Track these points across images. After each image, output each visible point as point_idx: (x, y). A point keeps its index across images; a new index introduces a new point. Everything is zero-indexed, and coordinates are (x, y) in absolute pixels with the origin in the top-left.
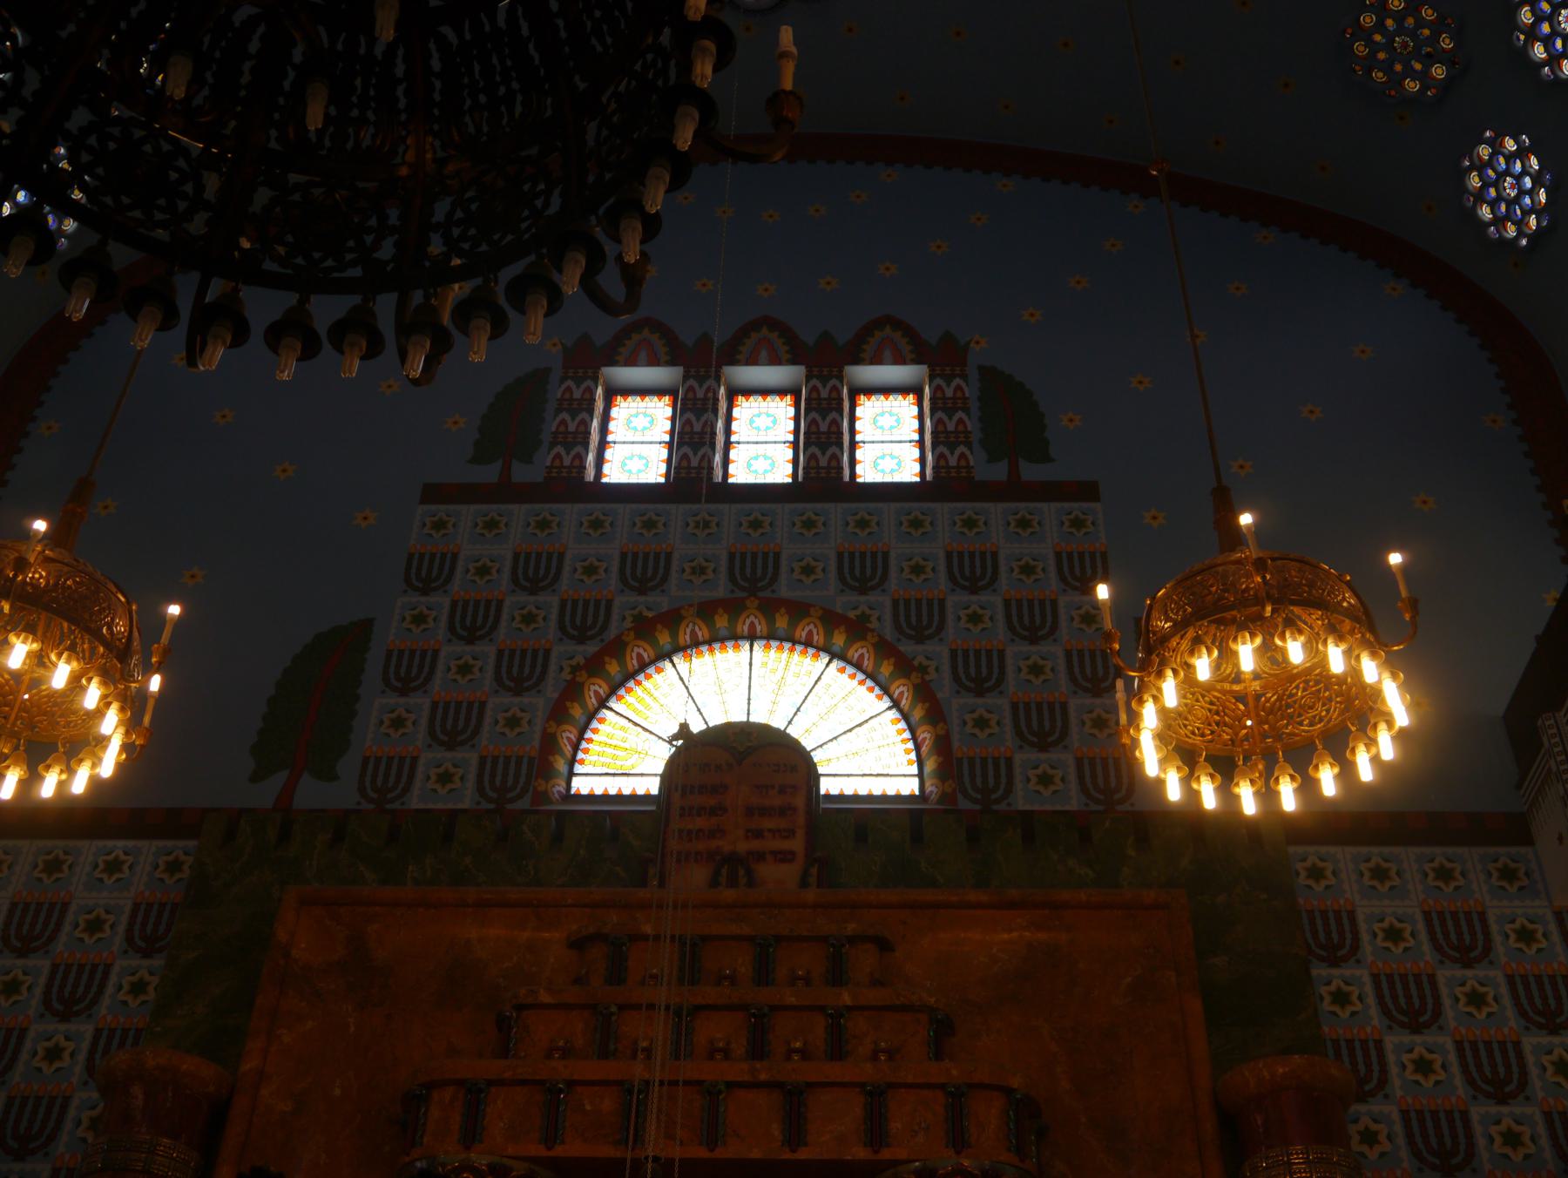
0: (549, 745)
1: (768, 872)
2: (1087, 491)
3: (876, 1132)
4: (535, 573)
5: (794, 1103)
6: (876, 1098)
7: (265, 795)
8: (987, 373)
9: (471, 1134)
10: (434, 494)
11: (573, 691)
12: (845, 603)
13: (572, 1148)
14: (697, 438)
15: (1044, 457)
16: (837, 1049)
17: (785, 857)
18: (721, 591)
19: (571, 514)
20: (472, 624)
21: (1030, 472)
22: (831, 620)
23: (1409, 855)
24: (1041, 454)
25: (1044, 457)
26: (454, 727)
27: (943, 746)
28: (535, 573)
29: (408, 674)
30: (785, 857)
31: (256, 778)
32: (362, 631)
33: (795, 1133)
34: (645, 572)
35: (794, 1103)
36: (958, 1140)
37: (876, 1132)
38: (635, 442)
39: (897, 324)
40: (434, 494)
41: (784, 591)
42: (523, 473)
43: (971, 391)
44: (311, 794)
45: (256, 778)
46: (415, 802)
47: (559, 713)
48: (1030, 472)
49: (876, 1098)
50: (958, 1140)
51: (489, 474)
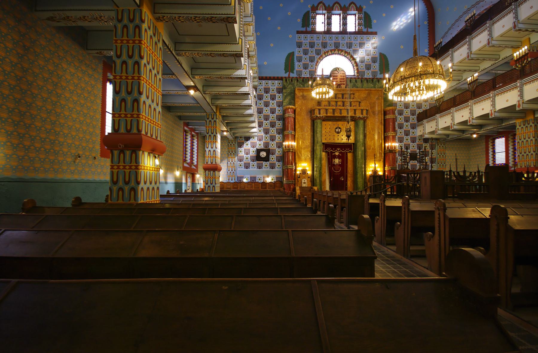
0: (316, 69)
1: (342, 86)
2: (375, 33)
4: (312, 45)
6: (355, 110)
7: (286, 75)
8: (365, 12)
9: (320, 114)
11: (317, 62)
15: (371, 28)
17: (344, 84)
18: (333, 48)
19: (315, 35)
20: (306, 52)
21: (370, 30)
22: (346, 52)
25: (371, 28)
26: (306, 67)
27: (358, 69)
28: (312, 45)
29: (299, 60)
30: (344, 84)
32: (293, 52)
34: (324, 45)
36: (362, 114)
37: (355, 114)
39: (354, 4)
40: (298, 32)
41: (340, 48)
42: (309, 29)
43: (363, 16)
44: (292, 75)
46: (303, 76)
47: (316, 65)
48: (370, 30)
49: (355, 110)
50: (362, 114)
51: (304, 29)
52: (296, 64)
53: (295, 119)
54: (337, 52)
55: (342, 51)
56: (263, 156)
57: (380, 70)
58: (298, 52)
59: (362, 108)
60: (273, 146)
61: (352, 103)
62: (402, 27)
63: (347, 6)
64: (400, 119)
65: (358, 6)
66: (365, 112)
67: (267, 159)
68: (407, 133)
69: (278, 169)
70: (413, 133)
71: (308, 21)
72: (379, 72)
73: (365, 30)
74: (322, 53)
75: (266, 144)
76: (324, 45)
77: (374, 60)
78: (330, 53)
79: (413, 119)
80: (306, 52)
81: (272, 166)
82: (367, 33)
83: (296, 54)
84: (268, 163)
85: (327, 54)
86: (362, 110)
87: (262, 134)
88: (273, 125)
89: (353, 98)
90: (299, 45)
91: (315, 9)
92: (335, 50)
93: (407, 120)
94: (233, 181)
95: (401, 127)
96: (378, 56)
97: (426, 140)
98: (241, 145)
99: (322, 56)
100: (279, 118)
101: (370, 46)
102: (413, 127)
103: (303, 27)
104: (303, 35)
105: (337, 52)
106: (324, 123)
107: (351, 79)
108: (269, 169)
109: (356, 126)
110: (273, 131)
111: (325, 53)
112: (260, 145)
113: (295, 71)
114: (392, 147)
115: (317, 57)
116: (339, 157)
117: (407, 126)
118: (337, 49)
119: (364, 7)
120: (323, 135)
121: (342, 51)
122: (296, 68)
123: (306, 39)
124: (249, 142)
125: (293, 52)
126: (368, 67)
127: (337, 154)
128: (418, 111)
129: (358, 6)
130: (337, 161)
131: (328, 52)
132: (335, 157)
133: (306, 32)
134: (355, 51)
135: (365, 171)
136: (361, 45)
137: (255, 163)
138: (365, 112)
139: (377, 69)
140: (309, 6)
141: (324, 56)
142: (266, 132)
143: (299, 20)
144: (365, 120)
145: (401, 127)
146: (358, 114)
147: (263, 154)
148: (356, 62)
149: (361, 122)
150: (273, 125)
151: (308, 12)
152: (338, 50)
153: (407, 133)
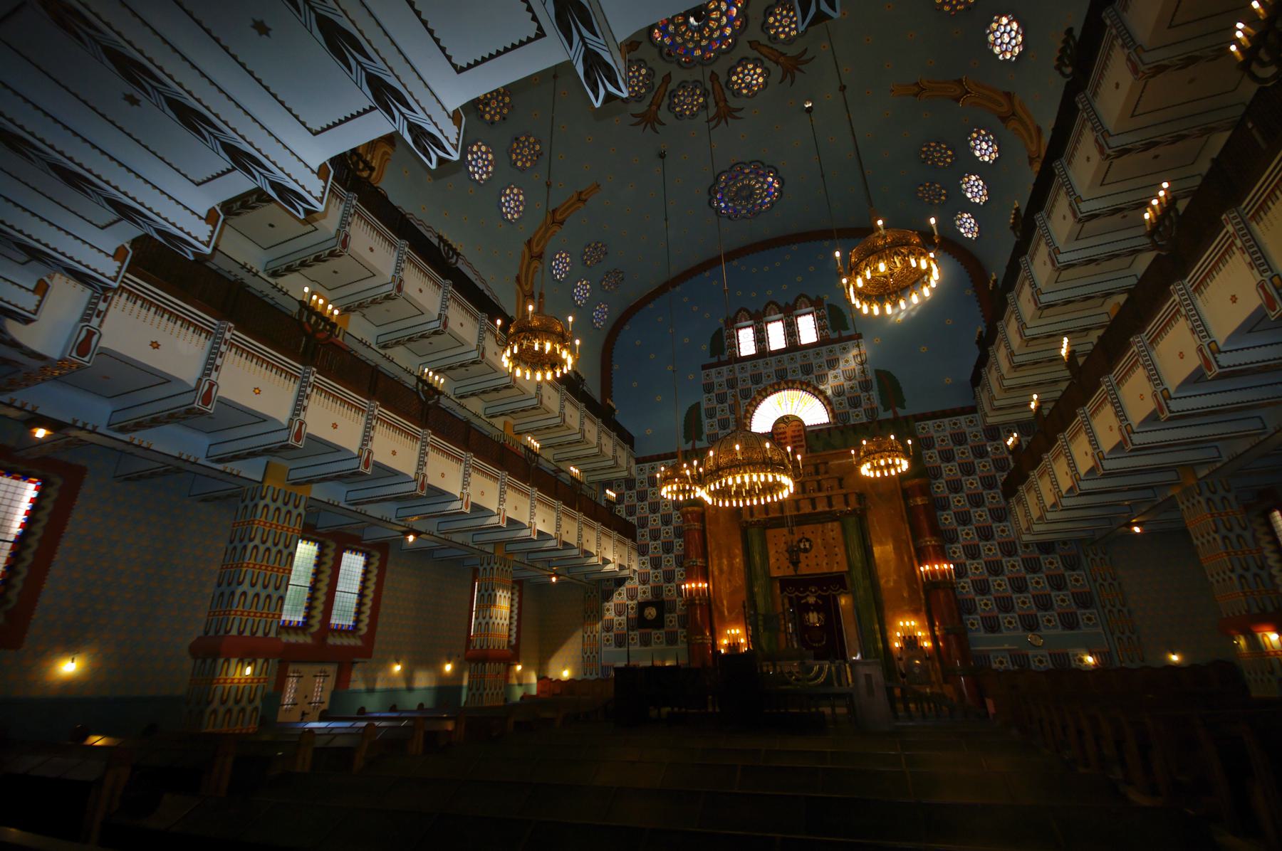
2: (859, 336)
3: (830, 505)
4: (732, 384)
5: (813, 502)
6: (829, 498)
7: (689, 447)
8: (829, 305)
10: (704, 367)
12: (804, 378)
13: (771, 515)
14: (761, 338)
15: (846, 328)
16: (820, 490)
21: (844, 333)
22: (802, 383)
23: (946, 420)
24: (846, 328)
27: (832, 411)
29: (711, 413)
31: (687, 442)
32: (697, 406)
33: (814, 507)
34: (757, 379)
35: (813, 502)
36: (847, 504)
37: (830, 505)
38: (746, 343)
40: (704, 367)
42: (724, 358)
45: (687, 442)
48: (844, 333)
49: (829, 498)
50: (847, 504)
51: (714, 360)
52: (706, 422)
53: (703, 532)
54: (783, 385)
55: (794, 382)
56: (649, 617)
57: (882, 403)
58: (705, 402)
59: (844, 491)
60: (668, 592)
61: (824, 482)
62: (913, 314)
63: (791, 303)
64: (958, 501)
65: (814, 298)
66: (853, 499)
67: (658, 623)
68: (986, 534)
69: (681, 646)
70: (1003, 531)
71: (723, 343)
72: (881, 409)
73: (835, 335)
74: (754, 394)
75: (657, 591)
76: (757, 379)
77: (865, 386)
78: (770, 390)
79: (993, 497)
80: (721, 399)
81: (671, 639)
82: (841, 340)
83: (704, 406)
84: (663, 631)
85: (764, 394)
86: (846, 496)
87: (648, 568)
88: (668, 548)
89: (826, 472)
90: (708, 388)
91: (733, 325)
92: (779, 384)
93: (976, 501)
94: (594, 677)
95: (964, 519)
96: (871, 375)
97: (1046, 547)
98: (608, 596)
99: (754, 399)
100: (679, 533)
101: (850, 361)
102: (1001, 515)
103: (712, 356)
104: (713, 370)
105: (783, 385)
106: (771, 533)
107: (818, 431)
108: (664, 646)
109: (844, 530)
110: (669, 561)
111: (759, 393)
112: (643, 592)
113: (704, 437)
114: (933, 573)
115: (744, 403)
116: (817, 608)
117: (981, 516)
118: (783, 382)
119: (826, 298)
120: (772, 561)
121: (794, 382)
122: (706, 430)
123: (719, 377)
124: (623, 589)
125: (698, 404)
126: (854, 402)
127: (812, 600)
128: (1001, 477)
129: (814, 298)
130: (813, 618)
131: (765, 390)
132: (807, 608)
133: (720, 364)
134: (822, 378)
135: (886, 641)
136: (832, 364)
137: (635, 634)
138: (853, 499)
139: (876, 401)
140: (721, 321)
141: (758, 398)
142: (656, 563)
143: (705, 347)
144: (861, 517)
145: (964, 519)
146: (838, 506)
147: (651, 613)
148: (826, 398)
149: (852, 521)
150: (668, 548)
151: (720, 332)
152: (787, 383)
153: (986, 534)
